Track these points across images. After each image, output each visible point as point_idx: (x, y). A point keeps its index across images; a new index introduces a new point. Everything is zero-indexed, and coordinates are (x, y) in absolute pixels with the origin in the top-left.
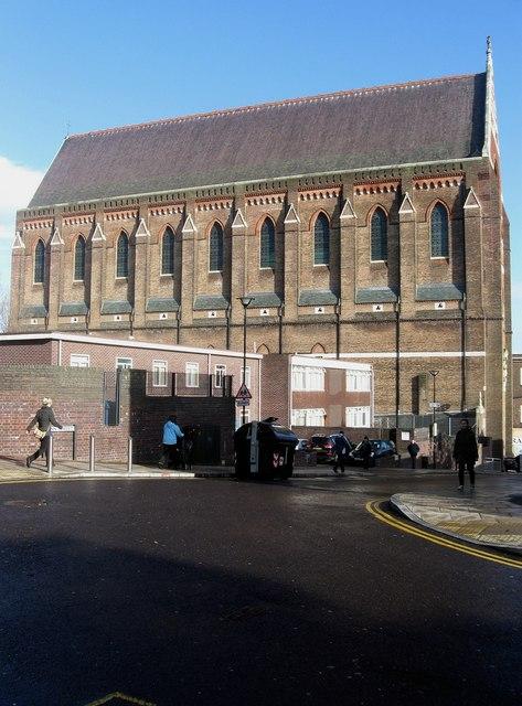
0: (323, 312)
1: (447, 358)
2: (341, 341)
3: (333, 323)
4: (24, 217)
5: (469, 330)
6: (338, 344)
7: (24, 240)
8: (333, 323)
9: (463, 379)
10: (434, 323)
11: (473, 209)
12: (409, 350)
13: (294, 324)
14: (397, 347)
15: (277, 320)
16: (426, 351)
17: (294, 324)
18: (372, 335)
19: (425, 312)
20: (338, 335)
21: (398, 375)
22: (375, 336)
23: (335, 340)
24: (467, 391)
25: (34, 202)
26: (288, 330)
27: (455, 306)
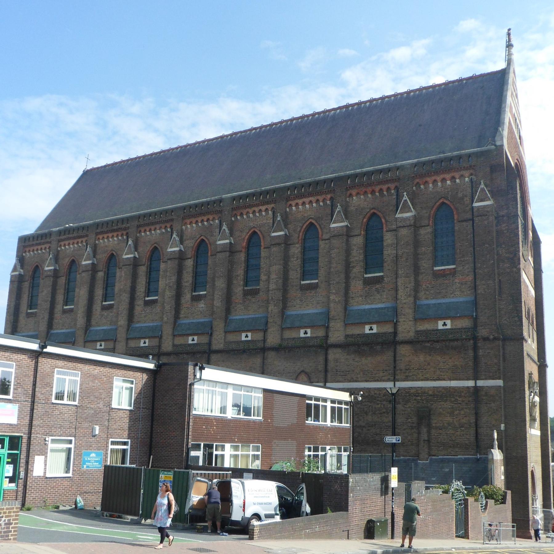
0: (309, 335)
1: (454, 388)
2: (329, 368)
3: (321, 346)
4: (25, 243)
5: (481, 352)
6: (326, 371)
7: (22, 267)
8: (321, 346)
9: (476, 414)
10: (438, 346)
11: (485, 206)
12: (406, 379)
13: (277, 349)
14: (395, 375)
15: (260, 345)
16: (427, 379)
17: (277, 349)
18: (364, 361)
19: (426, 332)
20: (326, 360)
21: (394, 408)
22: (368, 362)
23: (321, 367)
24: (480, 431)
25: (36, 231)
26: (271, 355)
27: (465, 323)
